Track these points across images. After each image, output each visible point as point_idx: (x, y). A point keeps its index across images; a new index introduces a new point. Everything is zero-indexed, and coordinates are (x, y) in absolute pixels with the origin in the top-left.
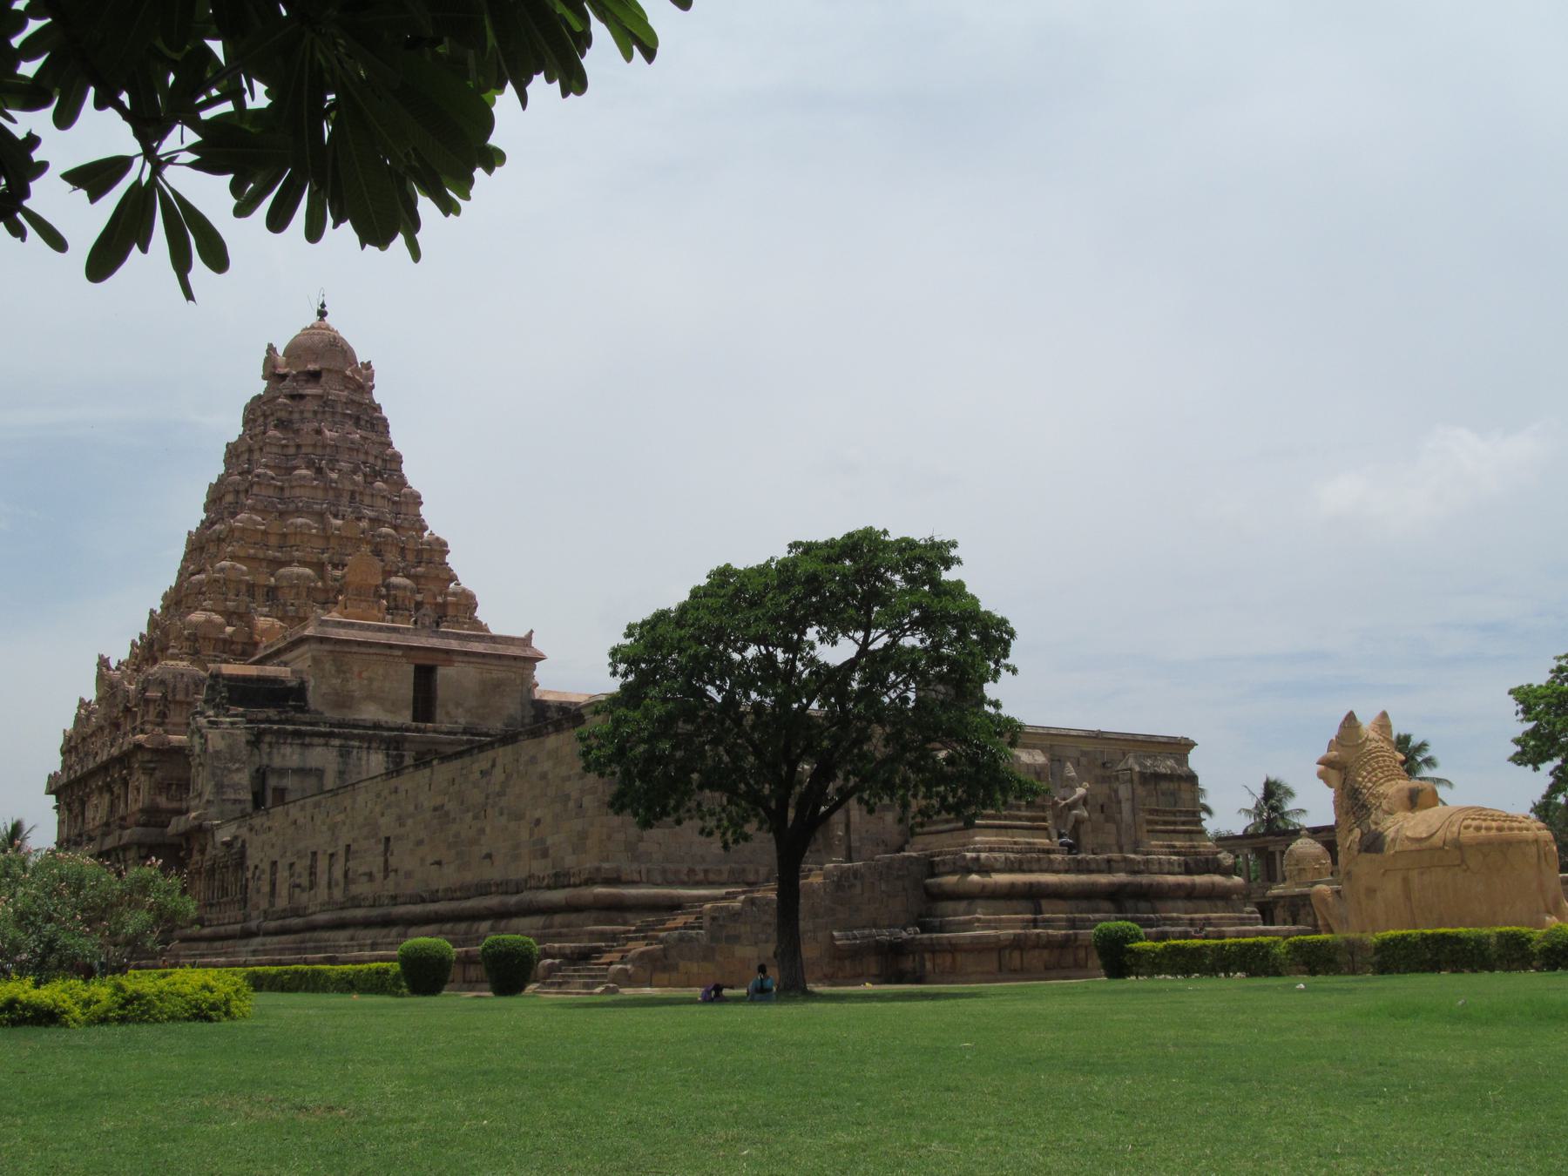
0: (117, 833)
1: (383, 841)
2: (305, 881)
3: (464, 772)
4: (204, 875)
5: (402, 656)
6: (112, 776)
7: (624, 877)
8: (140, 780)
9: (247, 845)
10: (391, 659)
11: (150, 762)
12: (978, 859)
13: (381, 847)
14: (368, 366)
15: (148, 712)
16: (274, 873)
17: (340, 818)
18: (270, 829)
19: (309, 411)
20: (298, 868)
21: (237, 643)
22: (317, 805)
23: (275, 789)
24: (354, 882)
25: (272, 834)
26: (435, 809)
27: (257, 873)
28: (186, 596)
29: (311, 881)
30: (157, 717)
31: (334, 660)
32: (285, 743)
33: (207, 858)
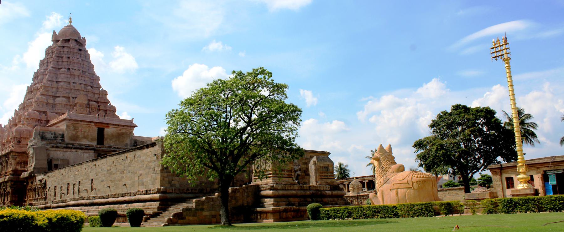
1: (91, 180)
2: (65, 192)
3: (117, 159)
4: (32, 190)
5: (94, 125)
6: (2, 160)
7: (168, 191)
8: (11, 161)
9: (47, 181)
10: (91, 126)
11: (15, 156)
12: (273, 186)
13: (90, 182)
14: (84, 38)
16: (55, 189)
17: (77, 173)
19: (66, 51)
20: (63, 188)
21: (43, 120)
22: (70, 170)
25: (55, 178)
26: (108, 171)
29: (67, 192)
30: (17, 142)
33: (33, 185)
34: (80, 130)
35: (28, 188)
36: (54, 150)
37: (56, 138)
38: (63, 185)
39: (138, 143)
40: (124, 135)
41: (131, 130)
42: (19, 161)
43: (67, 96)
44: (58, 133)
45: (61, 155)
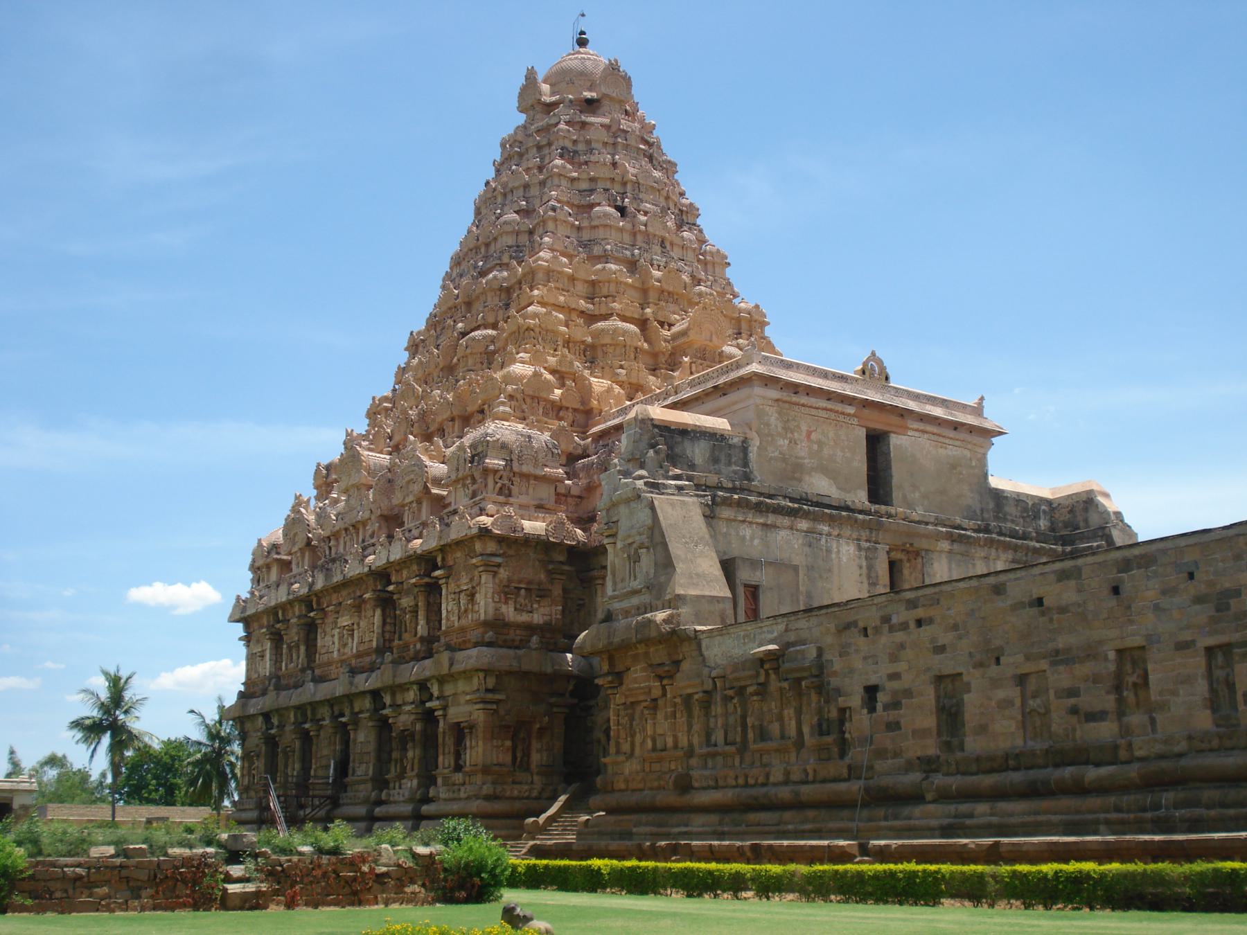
0: (445, 657)
4: (660, 716)
5: (854, 415)
9: (827, 656)
10: (841, 418)
15: (486, 486)
18: (919, 623)
21: (567, 408)
23: (746, 586)
25: (926, 631)
27: (882, 698)
29: (1120, 701)
31: (779, 414)
32: (744, 521)
34: (804, 434)
35: (619, 699)
36: (728, 520)
38: (1053, 664)
40: (959, 469)
41: (982, 451)
42: (510, 580)
43: (636, 316)
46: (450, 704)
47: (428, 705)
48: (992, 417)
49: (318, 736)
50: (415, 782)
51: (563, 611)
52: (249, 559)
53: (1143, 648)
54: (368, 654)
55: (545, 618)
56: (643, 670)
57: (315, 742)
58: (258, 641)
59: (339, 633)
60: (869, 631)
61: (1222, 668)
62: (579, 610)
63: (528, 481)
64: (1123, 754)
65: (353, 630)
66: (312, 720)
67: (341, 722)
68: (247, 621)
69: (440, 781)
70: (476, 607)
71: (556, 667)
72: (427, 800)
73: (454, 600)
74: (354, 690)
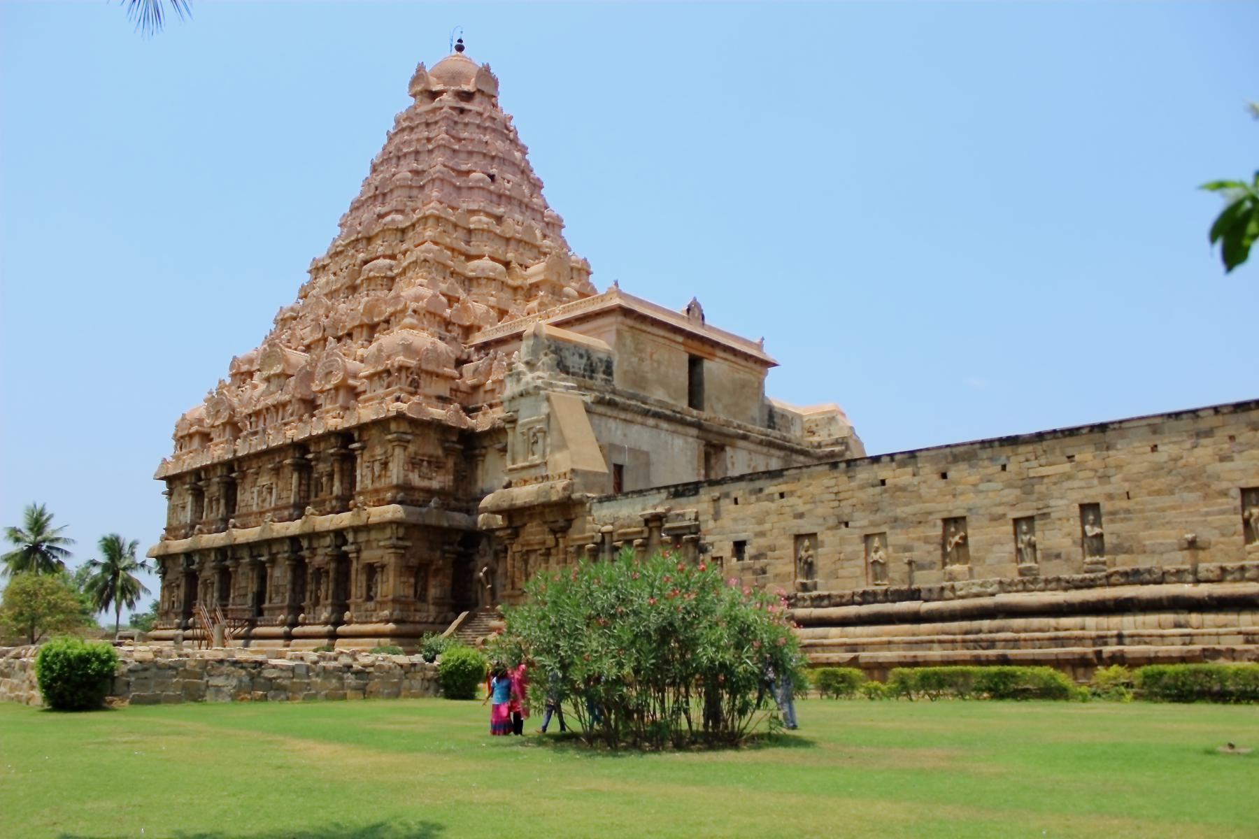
1: (1235, 493)
2: (927, 552)
4: (552, 560)
5: (682, 344)
18: (782, 495)
21: (454, 324)
24: (1117, 549)
27: (749, 550)
28: (369, 279)
29: (945, 555)
32: (610, 417)
35: (516, 547)
37: (591, 370)
39: (776, 420)
42: (416, 454)
44: (594, 358)
45: (619, 433)
46: (363, 548)
47: (344, 548)
48: (769, 353)
49: (236, 572)
50: (329, 609)
51: (455, 480)
52: (172, 431)
53: (962, 519)
54: (286, 508)
55: (442, 485)
56: (539, 525)
57: (233, 576)
58: (180, 495)
59: (258, 491)
60: (739, 500)
61: (1026, 534)
62: (462, 480)
63: (432, 377)
64: (947, 594)
65: (271, 489)
66: (231, 559)
67: (260, 561)
68: (171, 480)
69: (352, 607)
70: (389, 473)
71: (451, 523)
72: (343, 623)
73: (368, 467)
74: (275, 535)
